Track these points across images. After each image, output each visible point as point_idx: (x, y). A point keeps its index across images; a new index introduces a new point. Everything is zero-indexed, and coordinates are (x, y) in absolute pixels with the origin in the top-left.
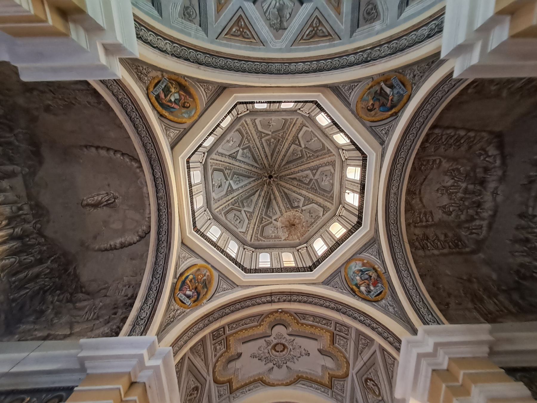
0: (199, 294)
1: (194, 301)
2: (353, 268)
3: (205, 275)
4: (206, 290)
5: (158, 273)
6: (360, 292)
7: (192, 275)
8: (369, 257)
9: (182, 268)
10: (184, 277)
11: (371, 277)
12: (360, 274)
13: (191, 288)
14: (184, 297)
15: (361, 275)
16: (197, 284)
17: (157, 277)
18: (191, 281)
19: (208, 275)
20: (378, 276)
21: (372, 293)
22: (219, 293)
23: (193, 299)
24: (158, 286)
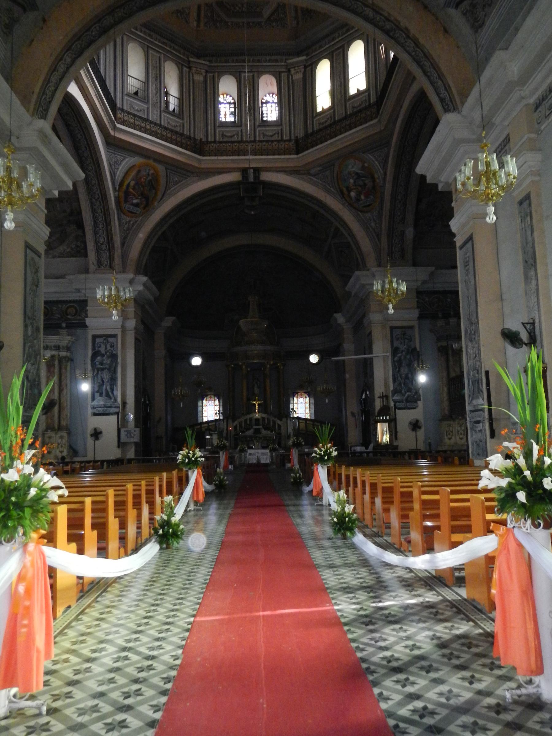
0: (147, 198)
1: (144, 208)
2: (350, 167)
3: (148, 175)
4: (154, 191)
5: (95, 193)
6: (349, 196)
7: (134, 180)
8: (373, 161)
9: (119, 176)
10: (124, 187)
11: (365, 185)
12: (355, 178)
13: (137, 195)
14: (132, 207)
15: (357, 179)
16: (142, 189)
17: (96, 198)
18: (134, 189)
19: (153, 174)
20: (374, 187)
21: (361, 202)
22: (172, 189)
23: (142, 206)
24: (101, 207)
